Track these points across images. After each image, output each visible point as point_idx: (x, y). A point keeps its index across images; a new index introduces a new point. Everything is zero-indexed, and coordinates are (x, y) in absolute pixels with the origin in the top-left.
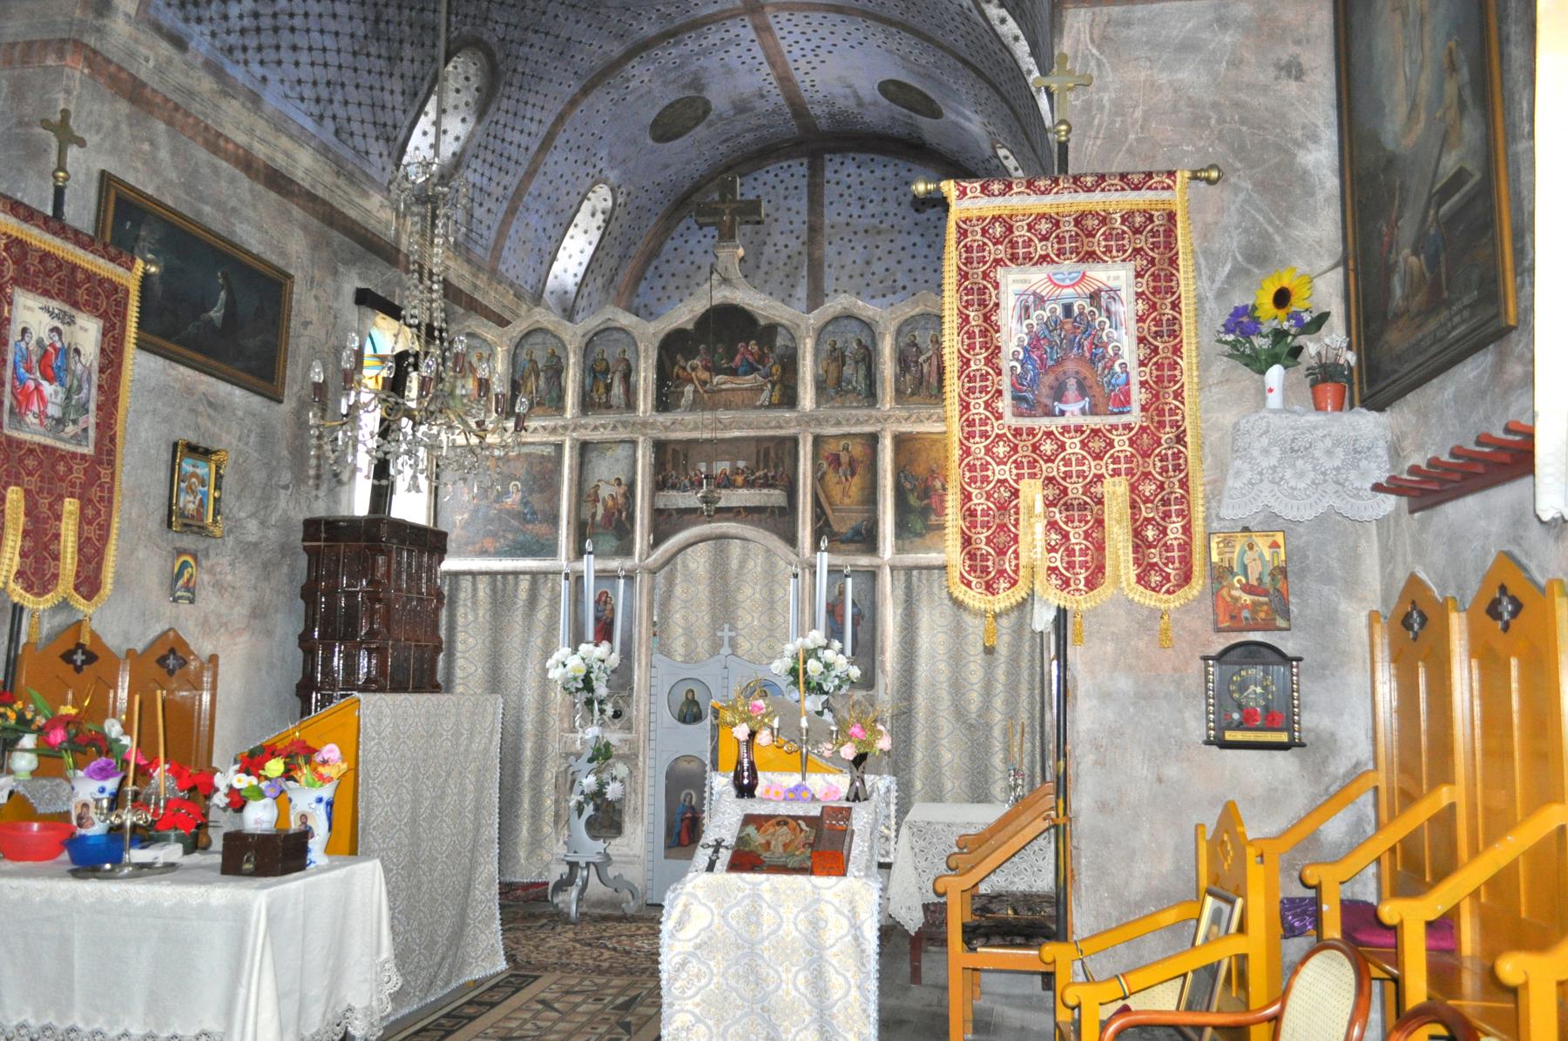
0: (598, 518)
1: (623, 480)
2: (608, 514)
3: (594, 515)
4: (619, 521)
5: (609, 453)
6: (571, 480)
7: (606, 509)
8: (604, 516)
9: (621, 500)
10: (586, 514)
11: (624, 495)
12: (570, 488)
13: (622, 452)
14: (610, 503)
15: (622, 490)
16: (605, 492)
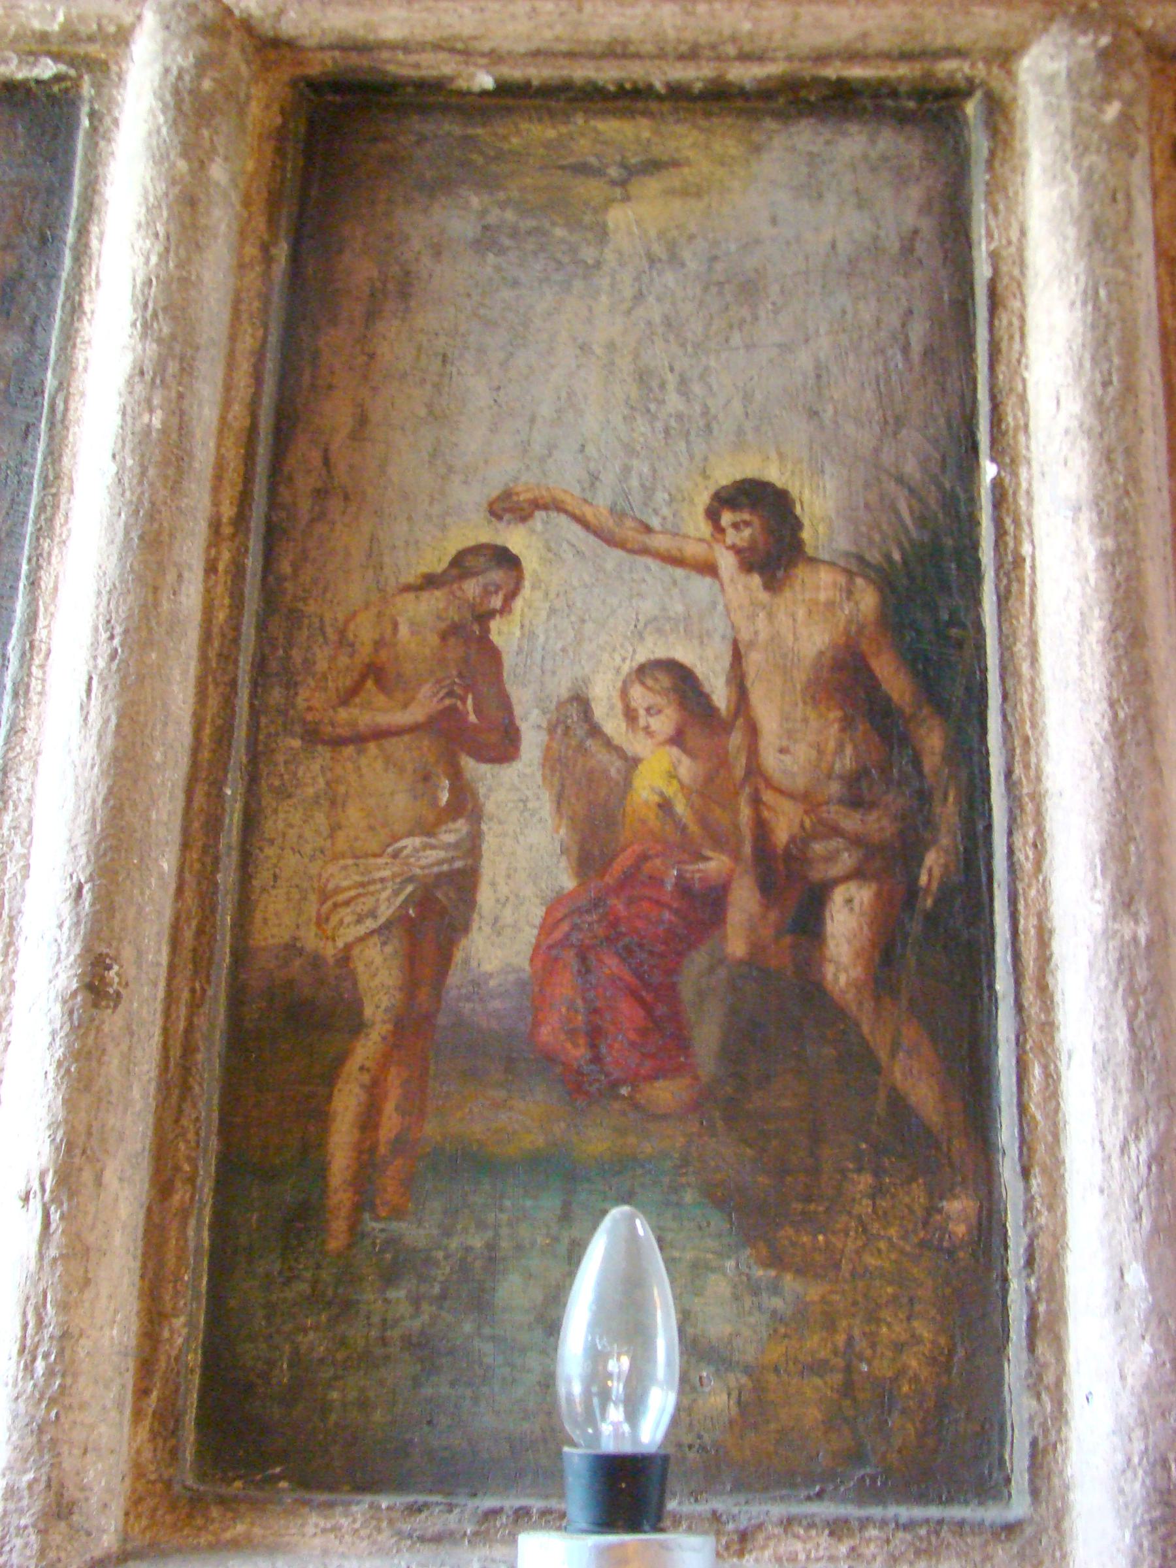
0: (500, 945)
1: (823, 508)
2: (632, 915)
3: (437, 915)
4: (787, 993)
5: (634, 219)
6: (159, 459)
7: (596, 830)
8: (569, 938)
9: (796, 743)
10: (337, 891)
11: (846, 681)
12: (149, 542)
13: (807, 206)
14: (659, 772)
15: (810, 619)
16: (588, 635)
